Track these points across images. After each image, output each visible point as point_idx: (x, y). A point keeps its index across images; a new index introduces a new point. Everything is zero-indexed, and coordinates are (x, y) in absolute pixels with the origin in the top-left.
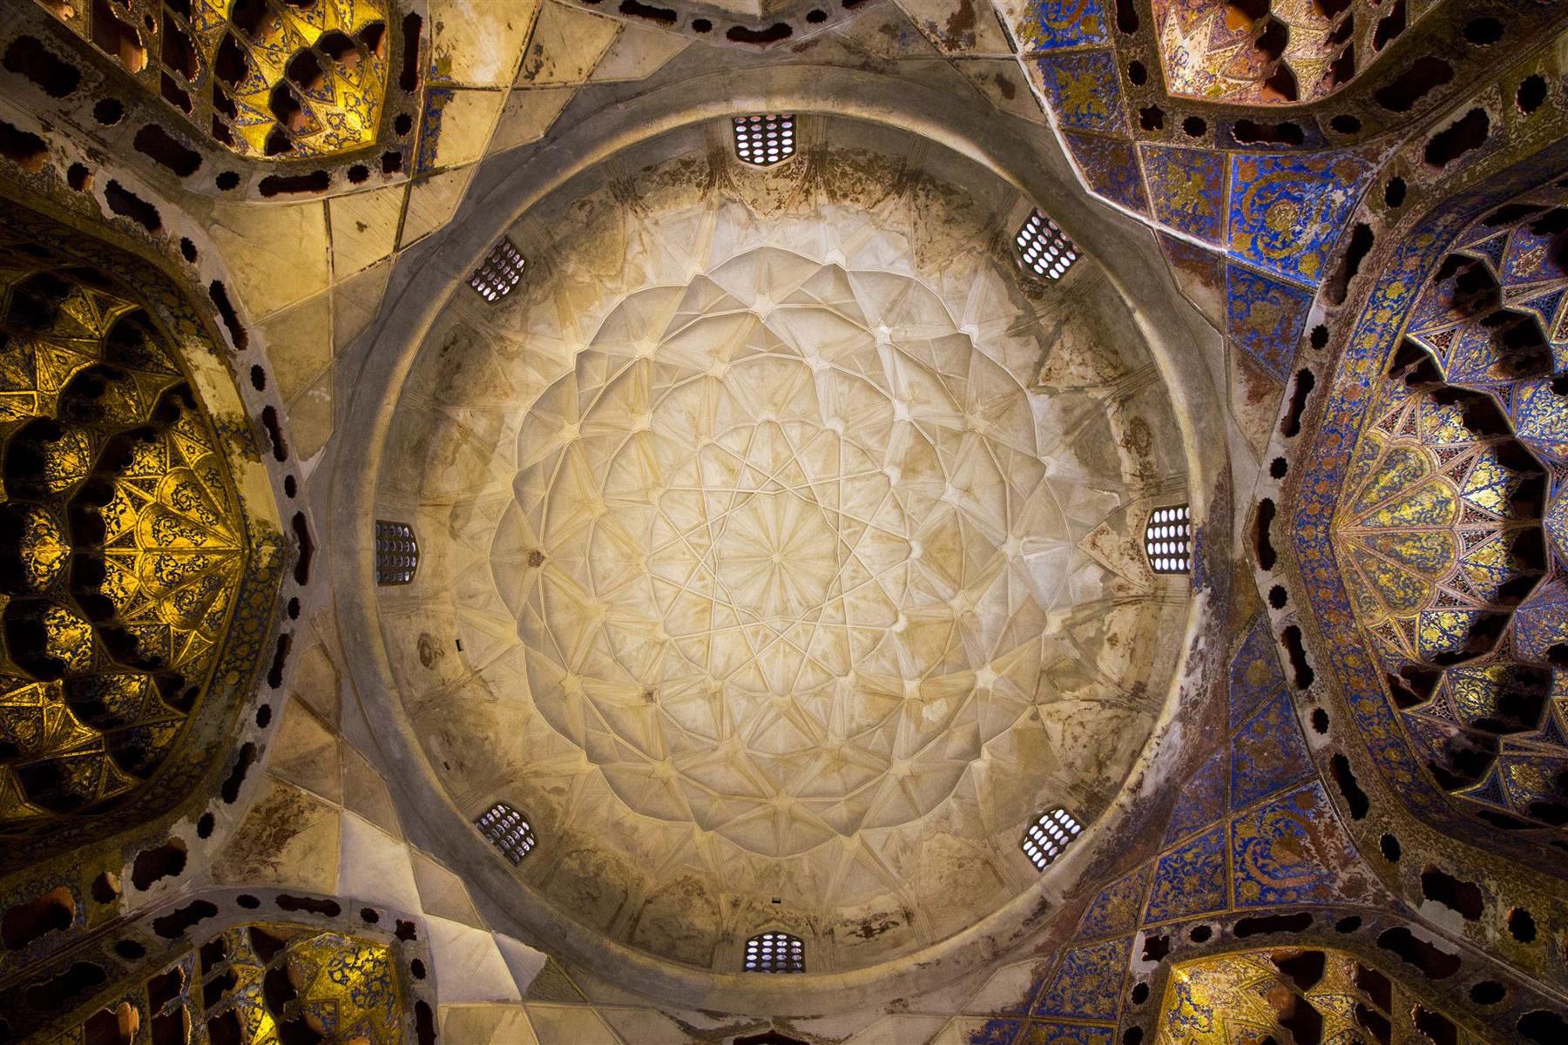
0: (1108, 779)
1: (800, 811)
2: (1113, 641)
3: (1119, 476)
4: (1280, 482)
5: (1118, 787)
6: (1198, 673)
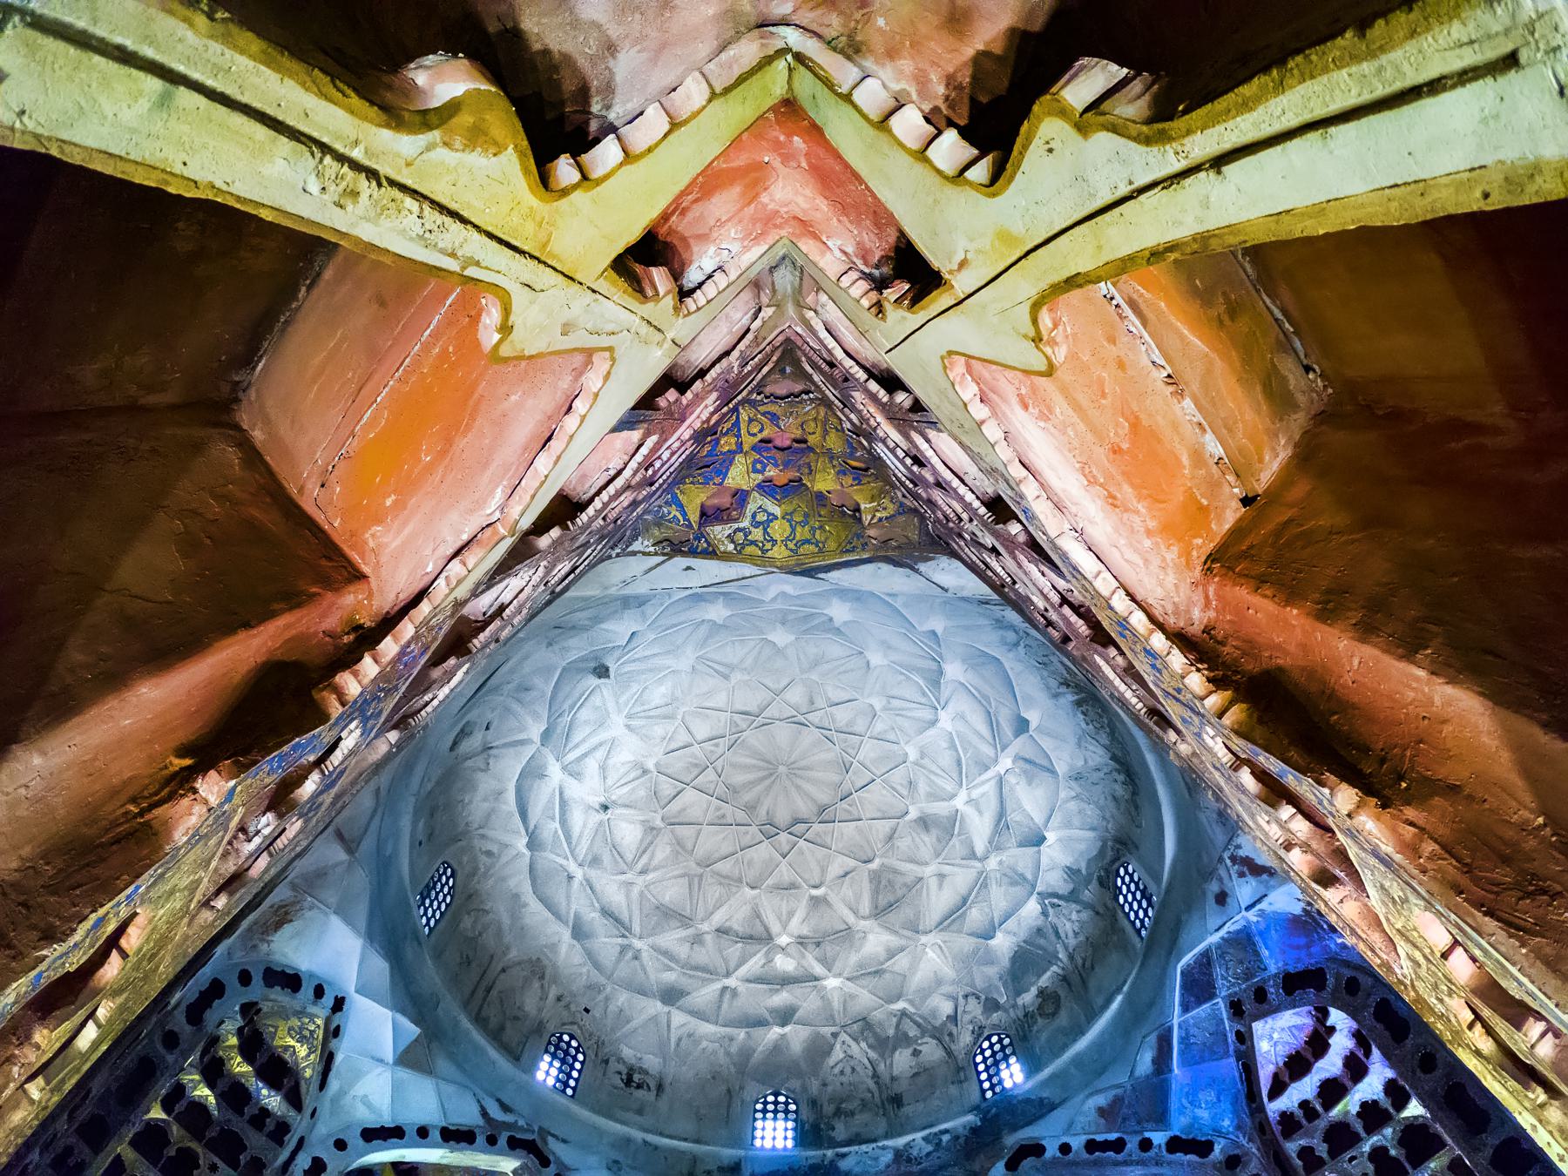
0: (833, 1129)
1: (644, 955)
2: (916, 1053)
3: (1018, 993)
4: (1058, 1154)
5: (833, 1144)
6: (930, 1148)
